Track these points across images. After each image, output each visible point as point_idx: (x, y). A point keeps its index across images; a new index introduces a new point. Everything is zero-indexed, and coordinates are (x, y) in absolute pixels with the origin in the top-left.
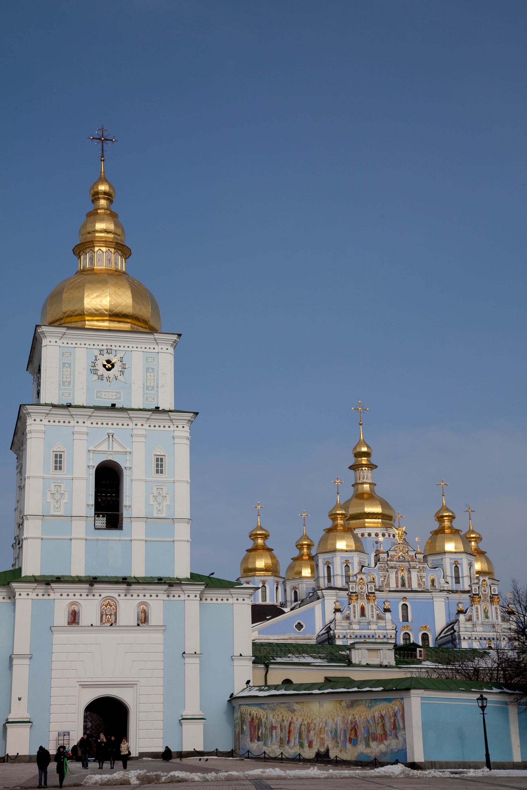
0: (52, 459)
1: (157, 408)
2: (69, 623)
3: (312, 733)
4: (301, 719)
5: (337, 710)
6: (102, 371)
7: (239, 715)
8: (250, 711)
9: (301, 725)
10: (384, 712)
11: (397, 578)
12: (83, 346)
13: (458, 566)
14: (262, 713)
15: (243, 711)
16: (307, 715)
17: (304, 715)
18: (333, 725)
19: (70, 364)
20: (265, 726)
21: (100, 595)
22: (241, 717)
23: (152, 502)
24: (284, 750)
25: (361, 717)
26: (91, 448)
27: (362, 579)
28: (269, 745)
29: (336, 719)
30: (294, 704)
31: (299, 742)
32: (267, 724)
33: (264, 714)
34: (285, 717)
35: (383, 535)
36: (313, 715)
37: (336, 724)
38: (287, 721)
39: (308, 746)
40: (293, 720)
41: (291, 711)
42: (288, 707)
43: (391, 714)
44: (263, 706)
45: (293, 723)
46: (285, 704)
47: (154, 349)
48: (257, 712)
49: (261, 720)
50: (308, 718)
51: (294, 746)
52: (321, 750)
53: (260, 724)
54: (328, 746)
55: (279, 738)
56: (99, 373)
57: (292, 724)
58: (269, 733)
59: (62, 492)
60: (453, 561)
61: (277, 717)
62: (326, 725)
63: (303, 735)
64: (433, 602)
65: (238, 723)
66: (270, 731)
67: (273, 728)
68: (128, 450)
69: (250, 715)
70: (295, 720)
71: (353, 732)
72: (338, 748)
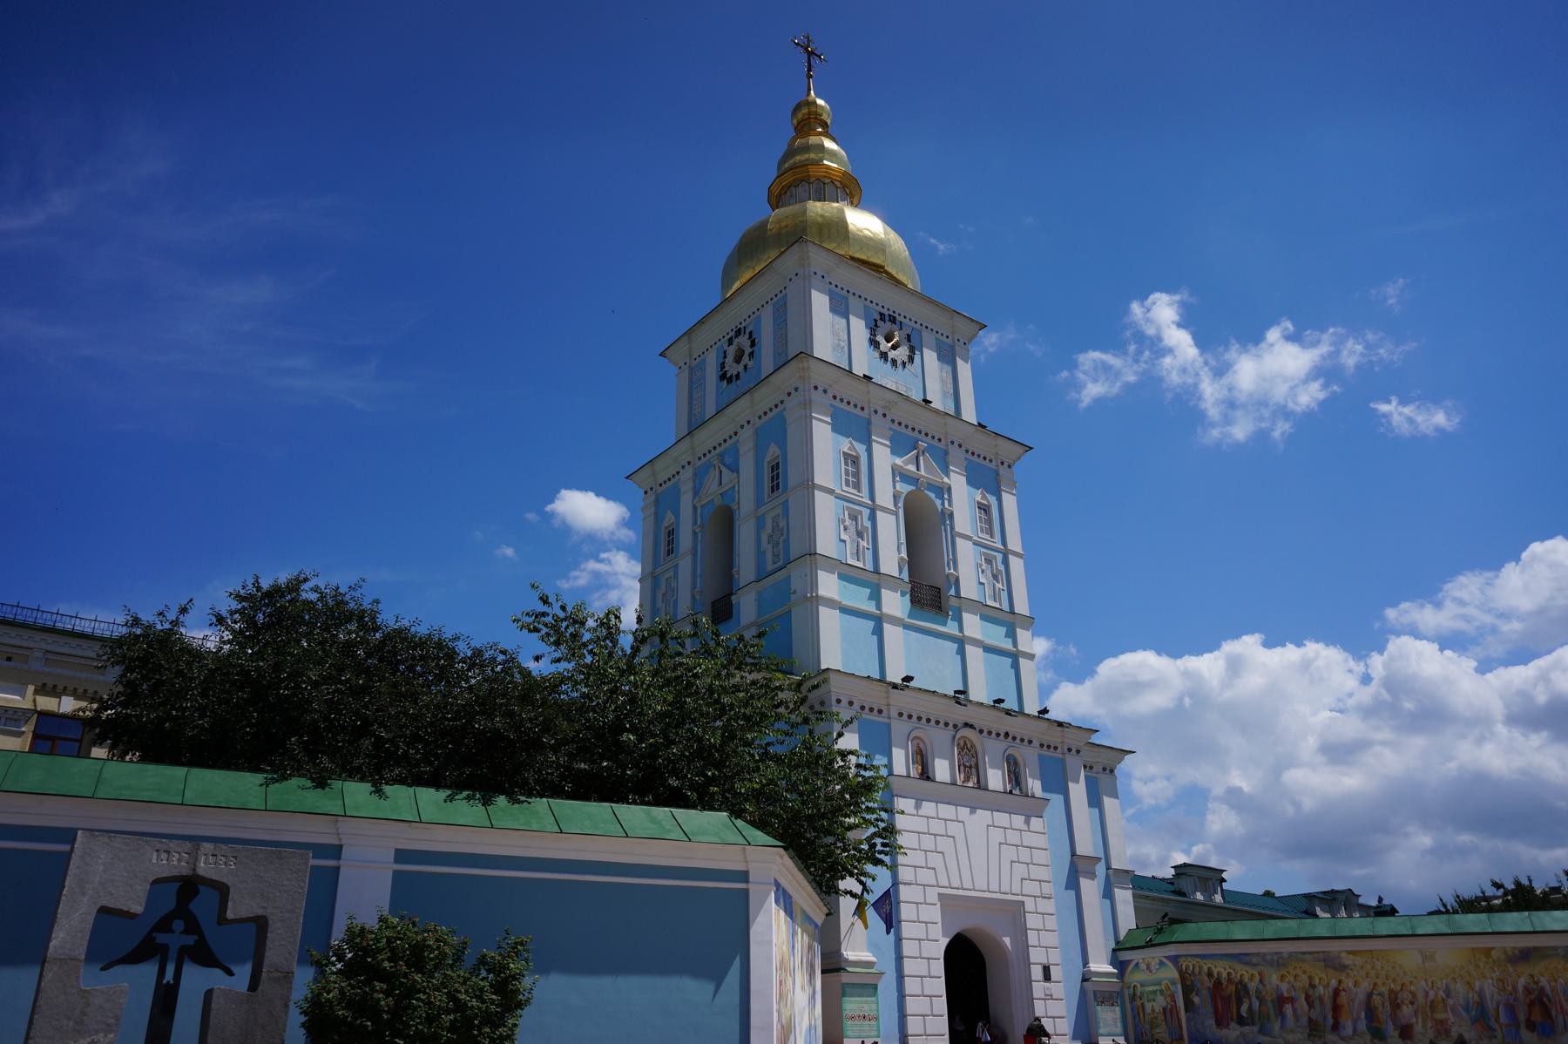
3: (1407, 1010)
4: (1366, 984)
5: (1477, 966)
7: (1171, 973)
8: (1209, 969)
9: (1369, 996)
15: (1187, 967)
16: (1387, 976)
17: (1377, 976)
18: (1471, 995)
20: (1257, 997)
22: (1183, 979)
25: (1556, 981)
29: (1477, 984)
30: (1343, 955)
31: (1369, 1028)
32: (1264, 993)
33: (1252, 975)
34: (1317, 981)
37: (1481, 993)
38: (1326, 986)
39: (1396, 1034)
41: (1335, 968)
45: (1344, 990)
47: (947, 337)
48: (1232, 971)
49: (1245, 986)
50: (1390, 981)
51: (1354, 1035)
53: (1242, 993)
55: (1304, 1021)
57: (1343, 993)
58: (1272, 1012)
61: (1292, 979)
63: (1380, 1015)
65: (1162, 992)
66: (1274, 1006)
67: (1281, 1001)
68: (946, 480)
69: (1210, 974)
70: (1351, 985)
72: (1494, 1040)
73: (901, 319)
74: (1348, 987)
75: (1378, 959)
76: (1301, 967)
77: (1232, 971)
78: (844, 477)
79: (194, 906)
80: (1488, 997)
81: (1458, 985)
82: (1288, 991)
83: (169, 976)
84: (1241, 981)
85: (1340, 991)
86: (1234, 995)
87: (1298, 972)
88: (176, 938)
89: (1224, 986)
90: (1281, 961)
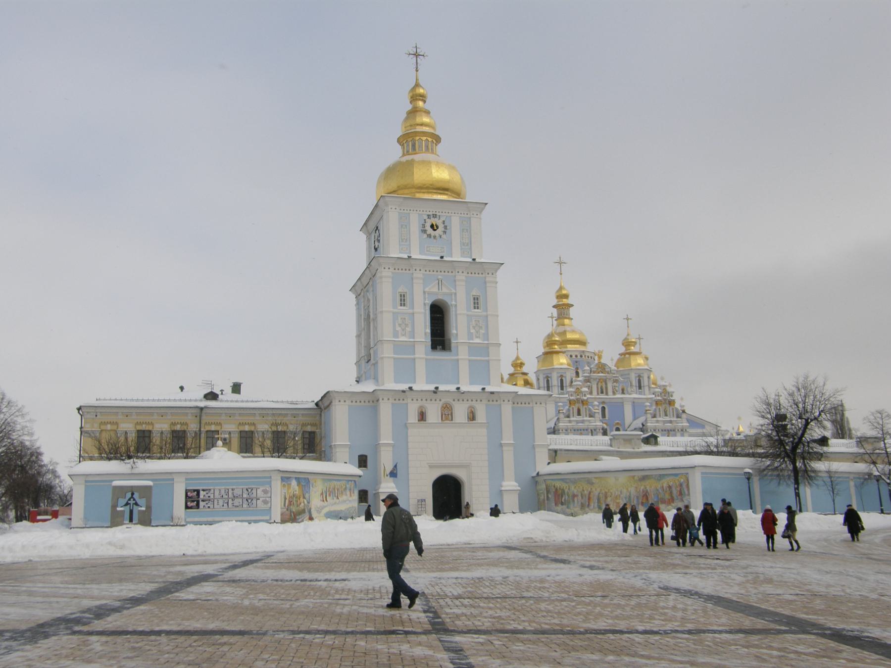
0: (398, 298)
1: (474, 260)
2: (419, 421)
3: (609, 499)
6: (430, 231)
7: (544, 486)
9: (599, 493)
10: (672, 483)
11: (598, 388)
12: (415, 211)
13: (641, 378)
19: (406, 226)
21: (440, 400)
22: (547, 488)
23: (472, 331)
26: (427, 290)
27: (578, 388)
29: (629, 489)
35: (581, 356)
37: (630, 494)
38: (587, 490)
43: (678, 484)
49: (564, 492)
55: (580, 503)
56: (428, 233)
59: (407, 323)
60: (637, 375)
64: (623, 406)
67: (574, 496)
69: (554, 486)
71: (645, 497)
73: (440, 214)
78: (398, 302)
79: (134, 496)
80: (632, 493)
83: (131, 508)
88: (132, 502)
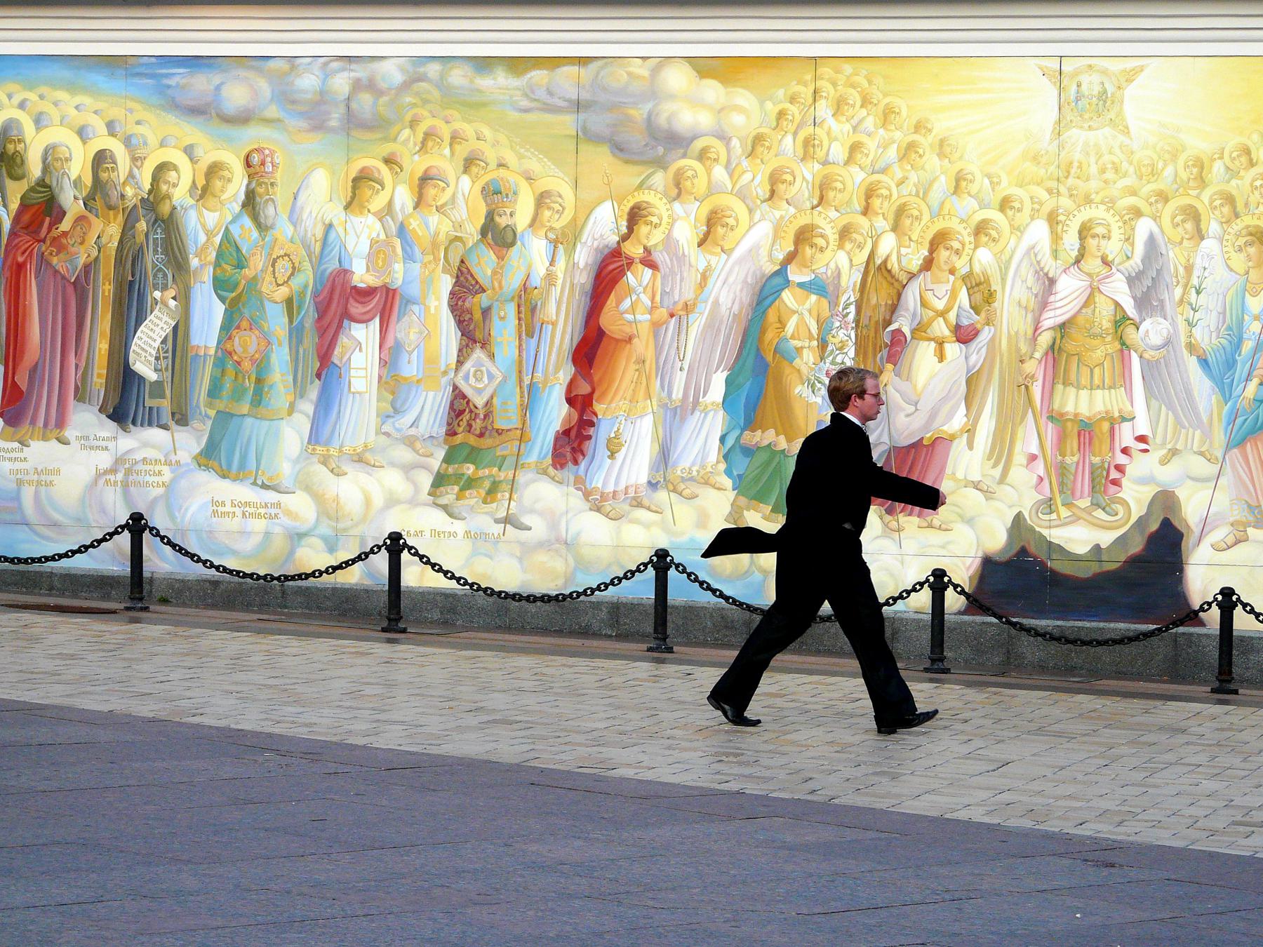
14: (189, 151)
16: (870, 194)
20: (220, 285)
24: (507, 520)
28: (285, 470)
30: (678, 79)
32: (257, 263)
33: (214, 170)
34: (521, 213)
36: (957, 187)
38: (564, 240)
40: (651, 236)
41: (619, 149)
42: (578, 106)
44: (200, 84)
46: (538, 76)
50: (881, 224)
51: (653, 485)
52: (1057, 535)
53: (152, 259)
54: (1166, 500)
57: (637, 278)
58: (280, 358)
61: (404, 197)
62: (1146, 302)
66: (296, 334)
70: (686, 233)
74: (669, 241)
75: (839, 106)
76: (455, 138)
77: (116, 147)
81: (1209, 245)
82: (377, 252)
84: (152, 203)
85: (630, 262)
86: (107, 270)
87: (443, 160)
89: (65, 225)
90: (365, 101)
